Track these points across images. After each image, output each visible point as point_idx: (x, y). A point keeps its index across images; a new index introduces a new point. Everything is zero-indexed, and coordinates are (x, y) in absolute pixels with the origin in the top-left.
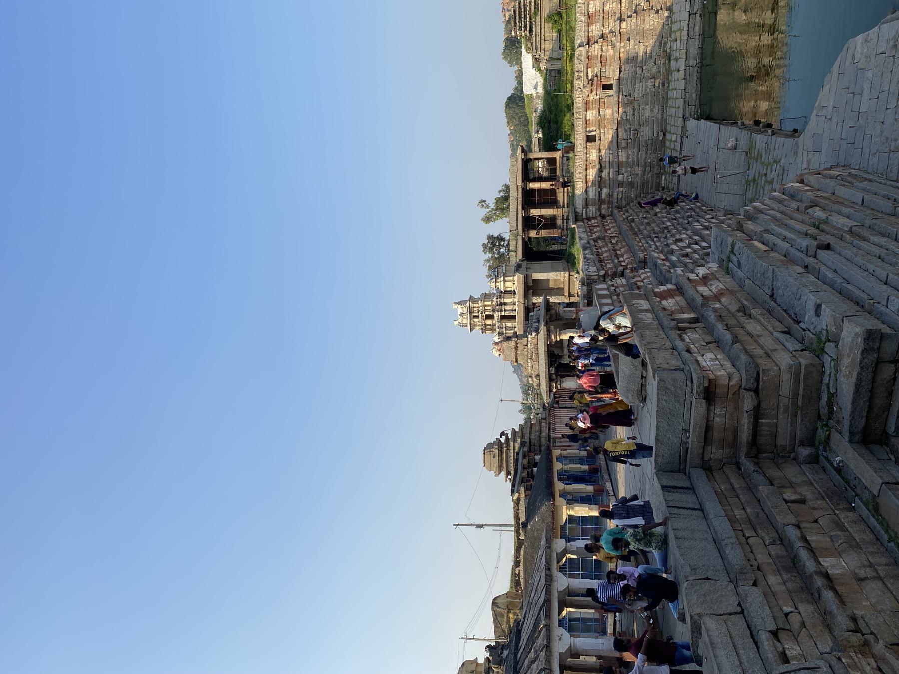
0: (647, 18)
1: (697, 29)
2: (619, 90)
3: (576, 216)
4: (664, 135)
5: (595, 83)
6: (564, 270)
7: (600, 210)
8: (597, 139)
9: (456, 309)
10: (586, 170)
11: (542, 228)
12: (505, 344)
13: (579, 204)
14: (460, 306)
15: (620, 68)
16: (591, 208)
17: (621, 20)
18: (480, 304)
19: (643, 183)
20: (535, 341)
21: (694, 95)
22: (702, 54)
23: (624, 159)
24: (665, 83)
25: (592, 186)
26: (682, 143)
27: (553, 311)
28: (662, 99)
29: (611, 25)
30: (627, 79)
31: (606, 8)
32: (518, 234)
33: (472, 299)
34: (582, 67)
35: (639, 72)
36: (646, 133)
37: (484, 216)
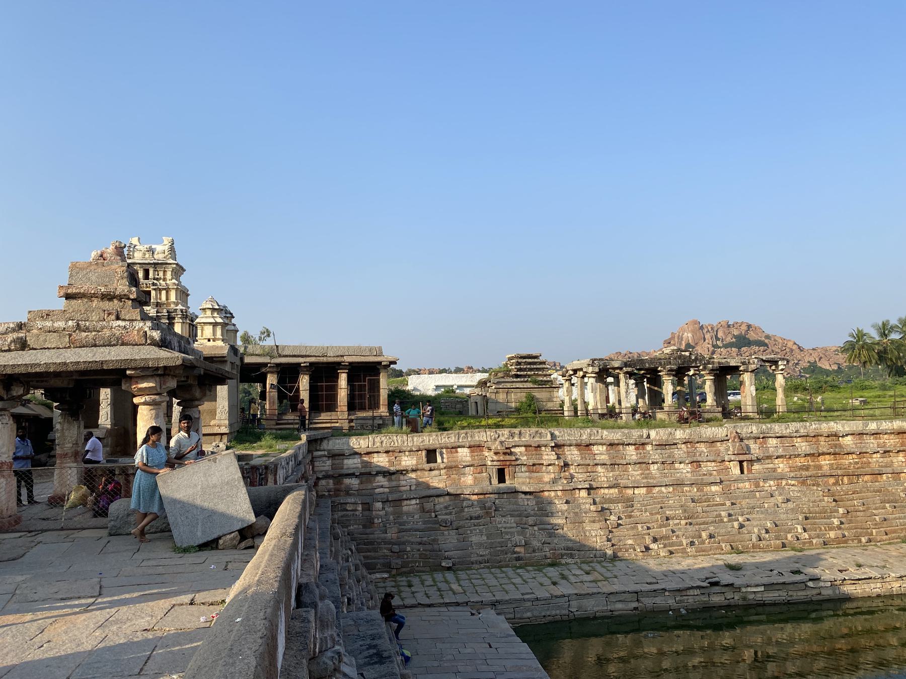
0: (597, 525)
1: (619, 606)
2: (499, 493)
3: (316, 440)
4: (449, 569)
5: (508, 457)
6: (231, 425)
7: (326, 477)
8: (432, 465)
9: (161, 242)
10: (387, 452)
11: (279, 391)
12: (119, 268)
13: (335, 444)
14: (166, 248)
15: (530, 493)
16: (329, 462)
17: (590, 489)
18: (171, 282)
19: (372, 543)
20: (135, 337)
21: (529, 614)
22: (588, 618)
23: (405, 509)
24: (520, 563)
25: (363, 462)
26: (458, 604)
27: (197, 394)
28: (501, 559)
29: (580, 476)
30: (516, 504)
31: (599, 468)
32: (272, 357)
33: (179, 271)
34: (526, 439)
35: (531, 520)
36: (449, 540)
37: (250, 334)
